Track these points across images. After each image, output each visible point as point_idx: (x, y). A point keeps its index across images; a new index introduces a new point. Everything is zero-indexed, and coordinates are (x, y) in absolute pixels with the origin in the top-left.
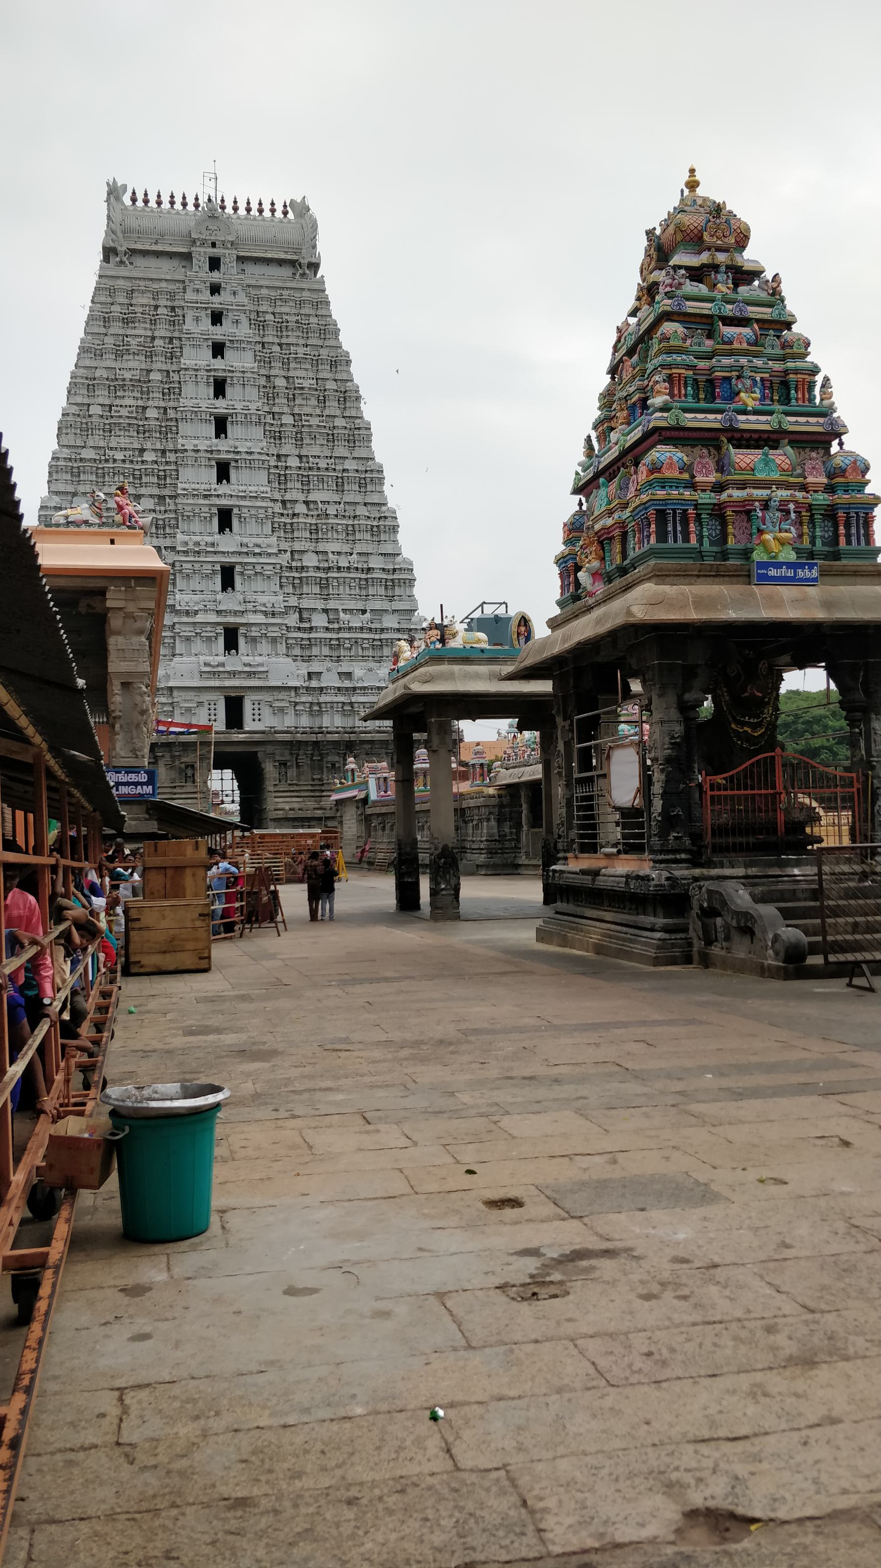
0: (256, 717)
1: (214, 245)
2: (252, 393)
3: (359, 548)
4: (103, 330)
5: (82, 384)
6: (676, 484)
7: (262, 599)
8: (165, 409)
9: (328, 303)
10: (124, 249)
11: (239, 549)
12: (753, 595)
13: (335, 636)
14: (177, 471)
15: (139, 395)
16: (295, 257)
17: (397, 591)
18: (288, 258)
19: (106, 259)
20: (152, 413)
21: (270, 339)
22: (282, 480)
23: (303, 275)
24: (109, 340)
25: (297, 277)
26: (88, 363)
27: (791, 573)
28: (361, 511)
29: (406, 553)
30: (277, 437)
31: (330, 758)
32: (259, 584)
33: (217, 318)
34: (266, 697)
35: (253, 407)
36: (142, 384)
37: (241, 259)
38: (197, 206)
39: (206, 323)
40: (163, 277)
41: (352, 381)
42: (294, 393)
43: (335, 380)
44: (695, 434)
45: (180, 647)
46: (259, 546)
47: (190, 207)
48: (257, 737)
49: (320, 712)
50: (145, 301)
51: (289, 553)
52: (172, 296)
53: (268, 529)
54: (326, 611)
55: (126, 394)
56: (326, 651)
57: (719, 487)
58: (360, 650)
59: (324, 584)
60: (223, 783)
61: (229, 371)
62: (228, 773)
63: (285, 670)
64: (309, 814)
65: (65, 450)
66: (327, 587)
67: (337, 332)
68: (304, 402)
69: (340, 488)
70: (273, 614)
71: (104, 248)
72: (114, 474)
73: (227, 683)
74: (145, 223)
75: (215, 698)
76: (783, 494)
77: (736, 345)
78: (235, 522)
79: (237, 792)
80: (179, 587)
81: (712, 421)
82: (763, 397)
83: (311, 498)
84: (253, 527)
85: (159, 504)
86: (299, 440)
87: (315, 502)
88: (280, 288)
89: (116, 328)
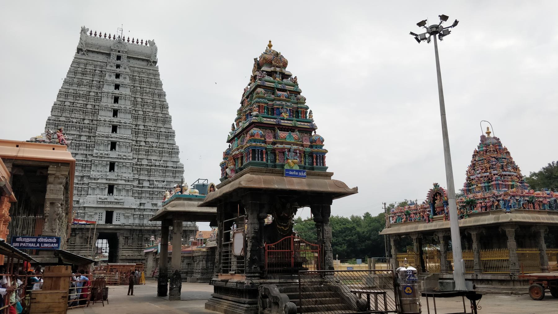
1: (119, 52)
2: (128, 103)
3: (164, 159)
4: (74, 76)
5: (63, 94)
6: (259, 141)
7: (124, 175)
8: (95, 107)
9: (159, 75)
11: (118, 157)
12: (284, 180)
13: (152, 190)
17: (177, 175)
18: (146, 59)
19: (78, 52)
20: (89, 106)
21: (137, 85)
22: (137, 133)
23: (151, 65)
24: (76, 80)
26: (66, 87)
27: (297, 174)
29: (181, 161)
30: (136, 118)
31: (146, 236)
32: (124, 170)
33: (118, 76)
34: (122, 212)
35: (128, 107)
36: (87, 96)
38: (114, 38)
39: (113, 77)
42: (144, 104)
44: (267, 125)
45: (90, 192)
46: (125, 156)
47: (112, 39)
48: (117, 227)
49: (143, 218)
50: (91, 68)
52: (101, 67)
53: (129, 150)
54: (149, 181)
56: (148, 195)
57: (274, 143)
59: (149, 171)
60: (103, 244)
62: (105, 241)
63: (131, 202)
64: (135, 258)
65: (54, 117)
67: (161, 85)
70: (128, 181)
71: (78, 49)
73: (107, 206)
74: (94, 42)
76: (295, 147)
77: (281, 98)
78: (117, 147)
79: (108, 249)
80: (92, 169)
81: (272, 121)
82: (290, 115)
83: (147, 140)
84: (124, 149)
86: (144, 120)
87: (148, 142)
89: (79, 76)
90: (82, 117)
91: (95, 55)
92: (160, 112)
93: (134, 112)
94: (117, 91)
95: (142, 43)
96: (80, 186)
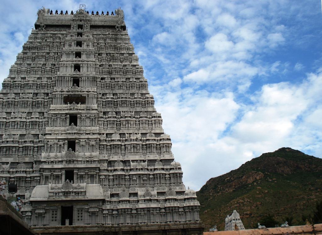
0: (80, 218)
14: (52, 101)
37: (93, 27)
51: (105, 135)
75: (55, 208)
87: (120, 112)
96: (28, 176)
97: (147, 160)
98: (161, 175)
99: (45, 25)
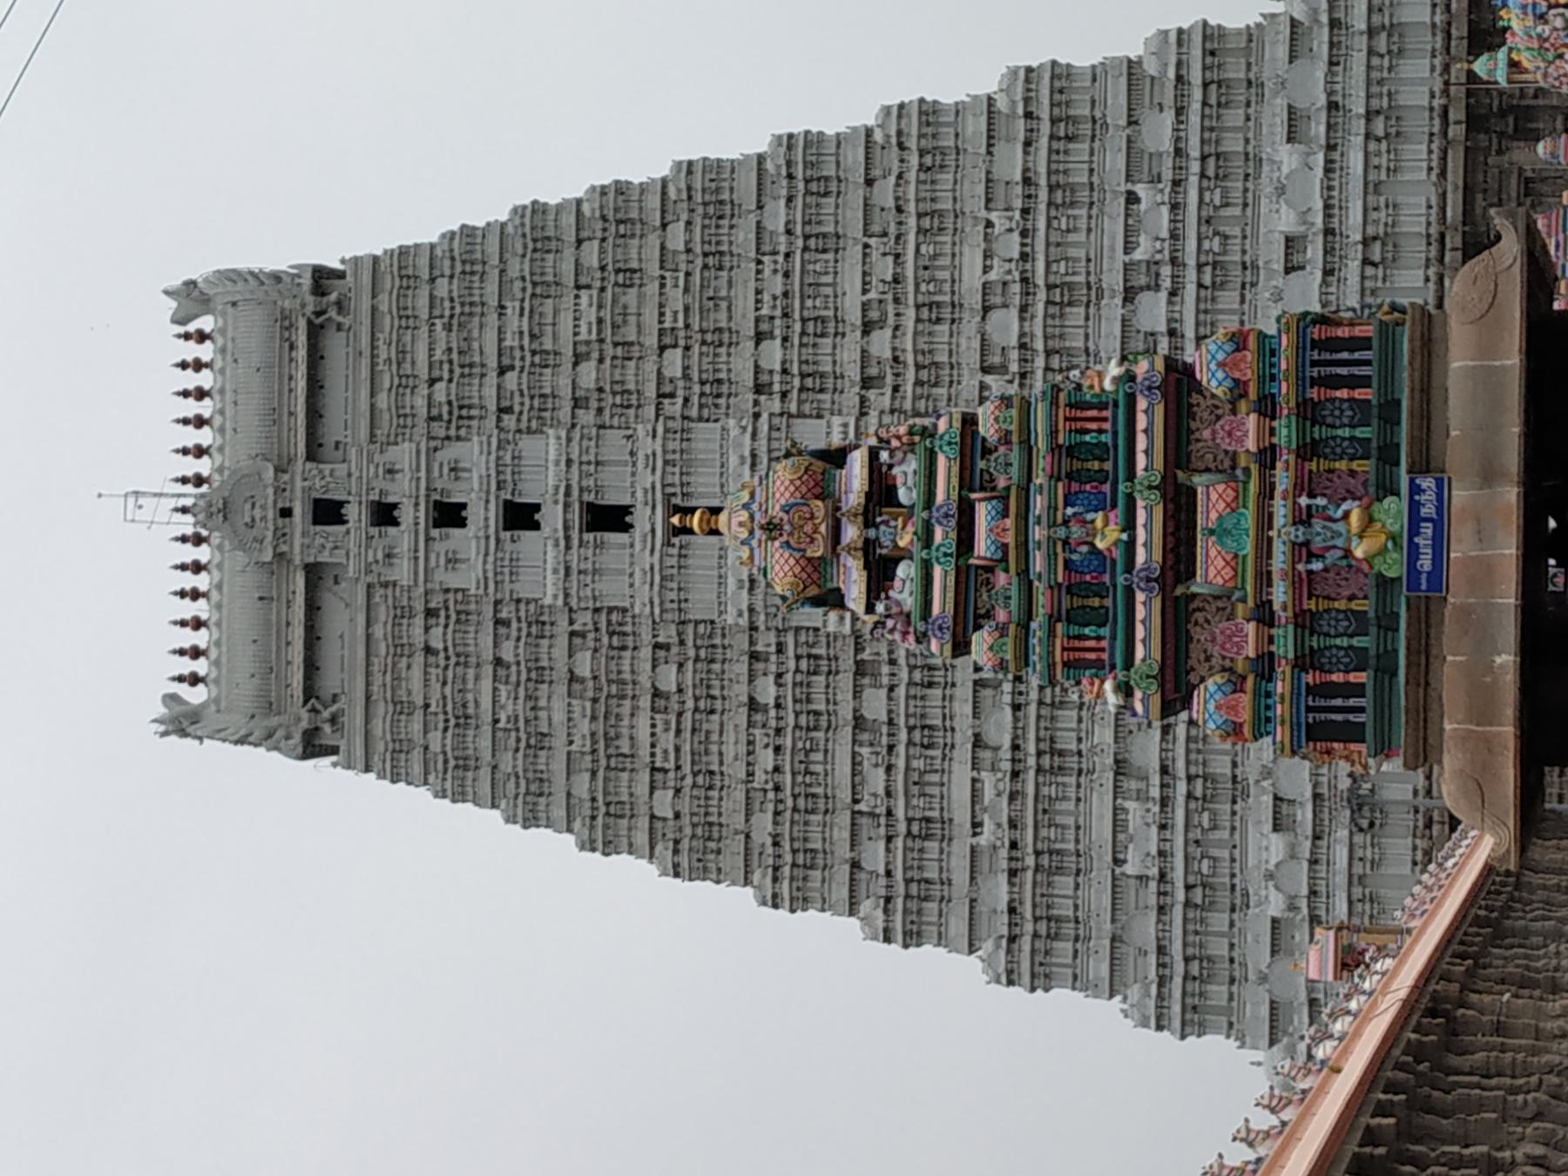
1: (286, 513)
9: (403, 251)
10: (304, 714)
14: (798, 630)
15: (627, 703)
16: (302, 324)
21: (490, 392)
25: (346, 321)
28: (885, 194)
29: (988, 83)
33: (449, 515)
37: (314, 452)
40: (361, 630)
41: (579, 202)
43: (579, 242)
50: (417, 673)
51: (989, 379)
54: (1129, 295)
55: (625, 731)
58: (1228, 212)
59: (1062, 296)
61: (568, 494)
65: (756, 877)
66: (1071, 286)
68: (632, 319)
69: (831, 244)
71: (305, 756)
72: (807, 772)
74: (246, 661)
83: (854, 316)
85: (876, 675)
87: (865, 307)
88: (373, 365)
90: (742, 719)
91: (332, 653)
92: (653, 240)
93: (674, 407)
94: (552, 517)
95: (198, 365)
97: (1130, 186)
98: (1207, 123)
99: (305, 702)
